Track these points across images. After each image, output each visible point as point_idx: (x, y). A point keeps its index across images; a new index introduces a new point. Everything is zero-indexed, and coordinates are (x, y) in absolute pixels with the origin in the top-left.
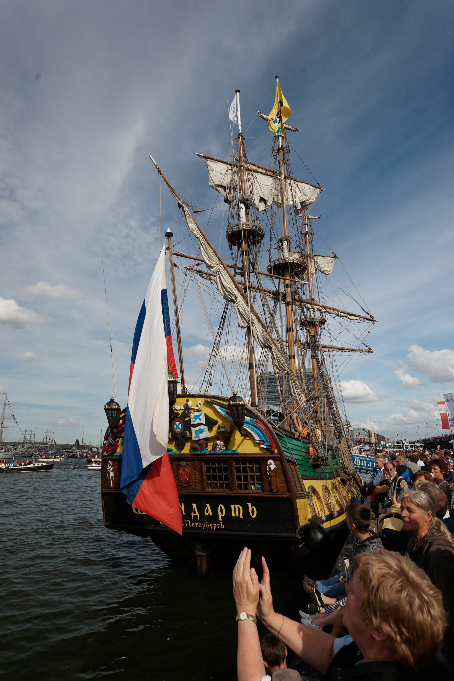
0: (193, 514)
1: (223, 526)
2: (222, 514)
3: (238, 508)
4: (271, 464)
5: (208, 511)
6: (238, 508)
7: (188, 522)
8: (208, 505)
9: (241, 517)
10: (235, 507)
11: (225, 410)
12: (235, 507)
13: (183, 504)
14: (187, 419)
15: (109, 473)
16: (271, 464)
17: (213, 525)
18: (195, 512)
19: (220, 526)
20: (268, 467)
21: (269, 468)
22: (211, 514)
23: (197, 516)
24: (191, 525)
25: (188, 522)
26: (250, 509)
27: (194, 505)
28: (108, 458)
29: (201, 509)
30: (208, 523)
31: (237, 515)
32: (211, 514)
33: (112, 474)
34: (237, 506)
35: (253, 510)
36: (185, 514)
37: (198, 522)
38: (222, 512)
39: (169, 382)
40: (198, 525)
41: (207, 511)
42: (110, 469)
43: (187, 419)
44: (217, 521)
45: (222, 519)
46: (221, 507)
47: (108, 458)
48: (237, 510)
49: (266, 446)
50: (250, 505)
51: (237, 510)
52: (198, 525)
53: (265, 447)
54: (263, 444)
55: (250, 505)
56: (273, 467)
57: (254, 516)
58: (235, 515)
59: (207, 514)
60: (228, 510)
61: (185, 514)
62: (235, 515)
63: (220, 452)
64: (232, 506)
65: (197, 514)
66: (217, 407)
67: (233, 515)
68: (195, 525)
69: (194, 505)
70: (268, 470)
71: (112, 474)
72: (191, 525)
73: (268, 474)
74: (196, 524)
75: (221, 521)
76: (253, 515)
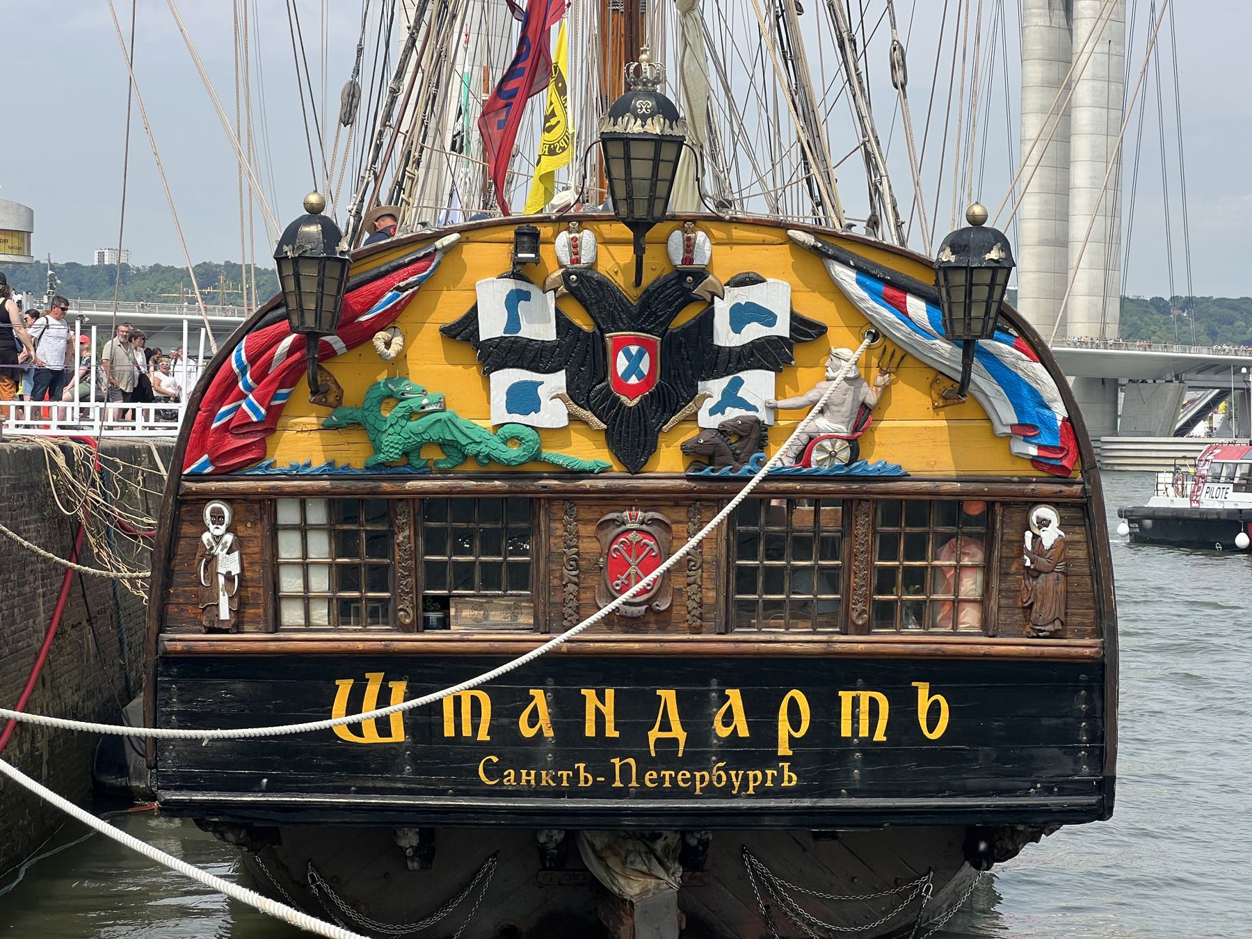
0: (654, 734)
1: (790, 779)
2: (797, 729)
3: (873, 703)
4: (1043, 523)
5: (733, 716)
6: (873, 703)
7: (626, 769)
8: (735, 696)
9: (880, 736)
10: (856, 702)
12: (856, 702)
13: (610, 693)
14: (687, 316)
15: (212, 560)
16: (1043, 523)
17: (745, 778)
18: (666, 726)
19: (778, 779)
20: (1028, 535)
21: (1035, 537)
22: (744, 732)
23: (675, 741)
24: (640, 778)
25: (626, 769)
26: (924, 703)
27: (668, 696)
28: (213, 485)
29: (695, 713)
30: (724, 769)
31: (864, 732)
32: (744, 732)
33: (230, 564)
34: (865, 696)
35: (934, 711)
36: (617, 734)
37: (677, 764)
38: (796, 725)
39: (606, 139)
40: (673, 780)
41: (728, 719)
42: (218, 539)
43: (687, 316)
44: (771, 759)
45: (791, 747)
46: (793, 700)
47: (213, 485)
48: (862, 714)
49: (1040, 447)
50: (923, 690)
51: (862, 714)
52: (673, 780)
53: (1033, 451)
54: (1027, 439)
55: (923, 690)
56: (1050, 536)
57: (935, 736)
58: (855, 731)
59: (724, 732)
60: (826, 711)
61: (617, 734)
62: (855, 731)
63: (826, 468)
64: (846, 697)
65: (678, 733)
66: (846, 276)
67: (846, 731)
68: (661, 780)
69: (668, 696)
70: (1028, 544)
71: (230, 564)
72: (640, 778)
73: (1028, 563)
74: (667, 773)
75: (785, 759)
76: (931, 730)
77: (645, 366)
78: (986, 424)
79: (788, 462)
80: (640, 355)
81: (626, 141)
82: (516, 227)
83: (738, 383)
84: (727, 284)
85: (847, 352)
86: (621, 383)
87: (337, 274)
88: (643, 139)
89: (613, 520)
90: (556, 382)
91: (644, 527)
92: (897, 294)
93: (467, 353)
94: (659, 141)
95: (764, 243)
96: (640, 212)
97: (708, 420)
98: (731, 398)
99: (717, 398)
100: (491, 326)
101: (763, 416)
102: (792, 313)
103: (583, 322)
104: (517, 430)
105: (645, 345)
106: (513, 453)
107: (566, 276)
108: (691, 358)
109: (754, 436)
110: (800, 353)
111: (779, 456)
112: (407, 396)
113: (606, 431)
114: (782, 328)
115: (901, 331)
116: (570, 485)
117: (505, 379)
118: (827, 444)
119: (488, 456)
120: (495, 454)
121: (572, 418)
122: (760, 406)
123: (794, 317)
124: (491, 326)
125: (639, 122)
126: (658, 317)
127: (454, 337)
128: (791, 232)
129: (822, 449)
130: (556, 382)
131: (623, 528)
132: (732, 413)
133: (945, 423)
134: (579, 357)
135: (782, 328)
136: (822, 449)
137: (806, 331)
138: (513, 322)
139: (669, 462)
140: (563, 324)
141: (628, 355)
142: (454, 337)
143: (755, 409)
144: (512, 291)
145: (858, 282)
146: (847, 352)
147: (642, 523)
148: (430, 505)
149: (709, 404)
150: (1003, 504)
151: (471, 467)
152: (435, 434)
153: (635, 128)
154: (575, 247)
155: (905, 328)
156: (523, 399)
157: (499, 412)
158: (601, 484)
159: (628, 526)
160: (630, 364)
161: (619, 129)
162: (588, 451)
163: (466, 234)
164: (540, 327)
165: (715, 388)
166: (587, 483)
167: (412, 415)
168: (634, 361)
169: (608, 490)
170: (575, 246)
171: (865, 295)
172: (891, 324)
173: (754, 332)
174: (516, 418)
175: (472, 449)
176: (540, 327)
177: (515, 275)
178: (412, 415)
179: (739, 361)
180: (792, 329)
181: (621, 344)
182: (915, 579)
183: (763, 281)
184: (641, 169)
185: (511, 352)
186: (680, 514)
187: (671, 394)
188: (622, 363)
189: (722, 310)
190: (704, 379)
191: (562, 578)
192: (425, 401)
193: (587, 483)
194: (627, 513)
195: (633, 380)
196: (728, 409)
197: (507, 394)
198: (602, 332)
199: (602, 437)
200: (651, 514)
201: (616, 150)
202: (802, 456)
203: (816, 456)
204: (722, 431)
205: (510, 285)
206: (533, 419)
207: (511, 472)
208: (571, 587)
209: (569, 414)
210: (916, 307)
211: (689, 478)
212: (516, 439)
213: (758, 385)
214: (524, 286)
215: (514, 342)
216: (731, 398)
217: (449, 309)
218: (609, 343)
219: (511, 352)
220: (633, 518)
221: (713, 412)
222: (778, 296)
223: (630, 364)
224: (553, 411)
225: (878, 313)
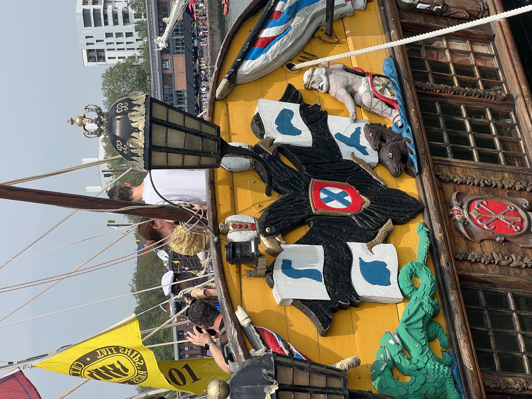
11: (256, 49)
66: (248, 66)
77: (337, 191)
78: (346, 21)
79: (395, 113)
80: (327, 192)
81: (151, 148)
82: (226, 263)
83: (339, 136)
84: (261, 136)
85: (308, 75)
86: (350, 207)
87: (290, 371)
88: (149, 134)
89: (464, 226)
90: (358, 249)
91: (465, 206)
92: (259, 43)
93: (342, 318)
94: (152, 122)
95: (227, 115)
96: (212, 146)
97: (372, 157)
98: (353, 141)
99: (353, 149)
100: (318, 291)
101: (362, 125)
102: (280, 101)
103: (302, 232)
104: (404, 275)
105: (319, 188)
106: (425, 280)
107: (266, 235)
108: (324, 159)
109: (379, 135)
110: (310, 100)
111: (393, 118)
112: (388, 357)
113: (395, 223)
114: (295, 108)
115: (287, 41)
116: (442, 247)
117: (361, 286)
118: (378, 88)
119: (433, 298)
120: (428, 291)
121: (386, 241)
122: (354, 126)
123: (284, 99)
124: (318, 291)
125: (134, 134)
126: (294, 177)
127: (330, 320)
128: (217, 95)
129: (382, 91)
130: (358, 249)
131: (468, 220)
132: (364, 141)
133: (349, 39)
134: (336, 235)
135: (295, 108)
136: (382, 91)
137: (291, 95)
138: (311, 274)
139: (409, 186)
140: (306, 240)
141: (329, 200)
142: (330, 320)
143: (358, 129)
144: (284, 272)
145: (254, 59)
146: (308, 75)
147: (461, 207)
148: (483, 359)
149: (359, 154)
150: (401, 18)
151: (442, 320)
152: (420, 335)
153: (140, 139)
154: (241, 227)
155: (285, 38)
156: (377, 273)
157: (391, 292)
158: (437, 226)
159: (466, 216)
160: (336, 199)
161: (141, 153)
162: (415, 237)
163: (235, 298)
164: (315, 256)
165: (346, 152)
166: (438, 236)
167: (405, 350)
168: (332, 197)
169: (441, 221)
170: (240, 227)
171: (262, 57)
172: (282, 45)
173: (297, 121)
174: (393, 278)
175: (428, 308)
176: (315, 256)
177: (270, 270)
178: (405, 350)
179: (324, 134)
180: (293, 101)
181: (320, 204)
182: (464, 70)
183: (258, 114)
184: (176, 139)
185: (337, 272)
186: (449, 188)
187: (354, 176)
188: (335, 204)
189: (281, 139)
190: (341, 156)
191: (519, 267)
192: (392, 342)
193: (438, 236)
194: (457, 217)
195: (349, 198)
196: (361, 144)
197: (374, 283)
198: (311, 215)
199: (399, 228)
200: (455, 202)
201: (159, 157)
202: (390, 104)
203: (388, 94)
204: (379, 150)
205: (278, 274)
206: (392, 266)
207: (439, 290)
208: (527, 260)
209: (383, 243)
210: (267, 33)
211: (420, 173)
212: (413, 276)
213: (338, 125)
214: (279, 264)
215: (329, 275)
216: (353, 141)
217: (304, 326)
218: (320, 211)
219: (337, 272)
220: (459, 213)
221: (366, 153)
222: (269, 108)
223: (336, 199)
224: (384, 253)
225: (276, 51)
